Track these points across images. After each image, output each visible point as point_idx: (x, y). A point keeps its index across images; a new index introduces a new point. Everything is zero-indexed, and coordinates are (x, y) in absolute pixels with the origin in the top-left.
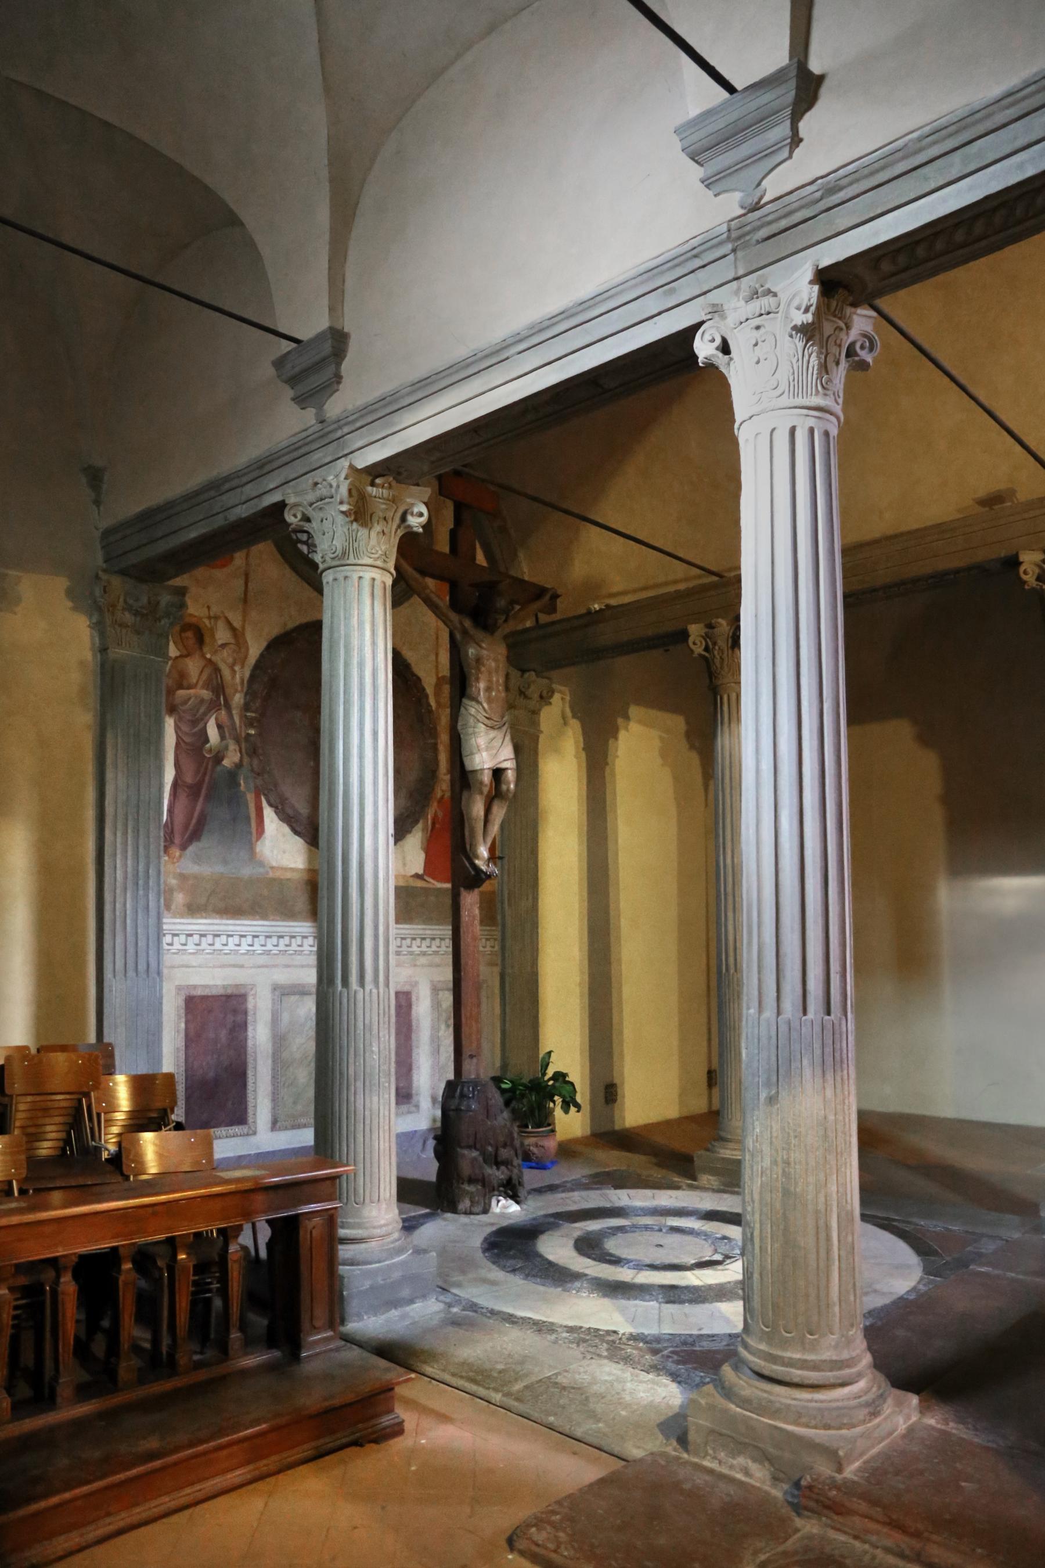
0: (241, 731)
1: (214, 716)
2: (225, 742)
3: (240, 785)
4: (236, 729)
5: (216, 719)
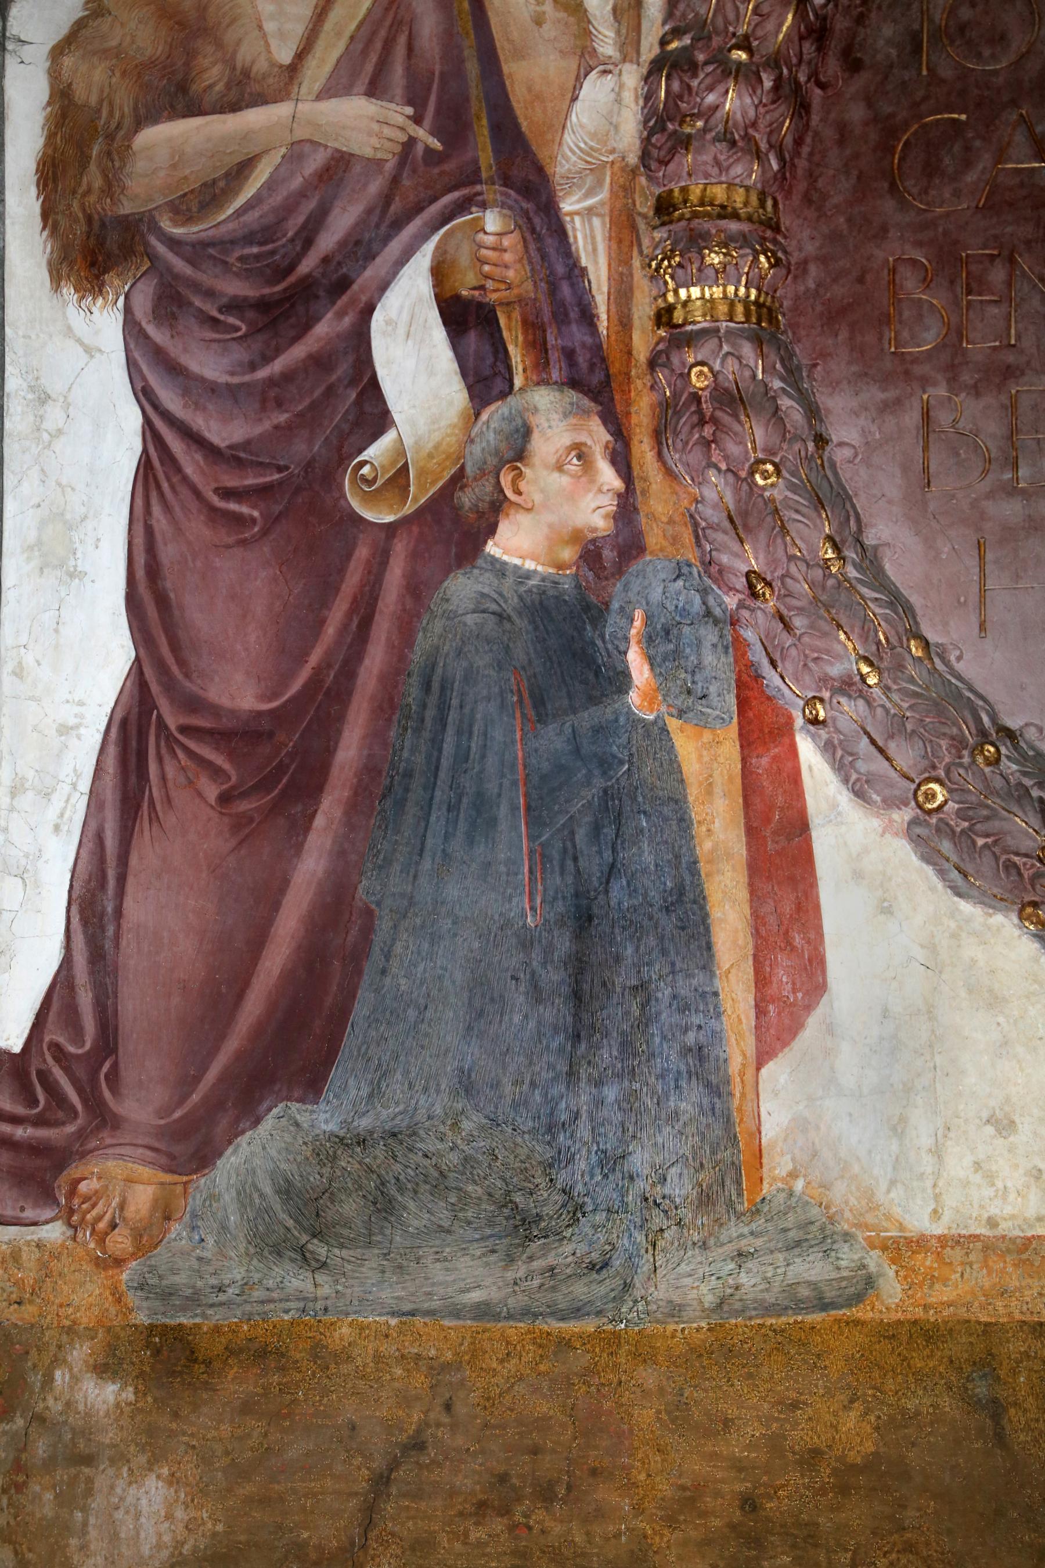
0: (624, 323)
1: (428, 250)
2: (495, 413)
3: (622, 680)
4: (588, 318)
5: (439, 273)
